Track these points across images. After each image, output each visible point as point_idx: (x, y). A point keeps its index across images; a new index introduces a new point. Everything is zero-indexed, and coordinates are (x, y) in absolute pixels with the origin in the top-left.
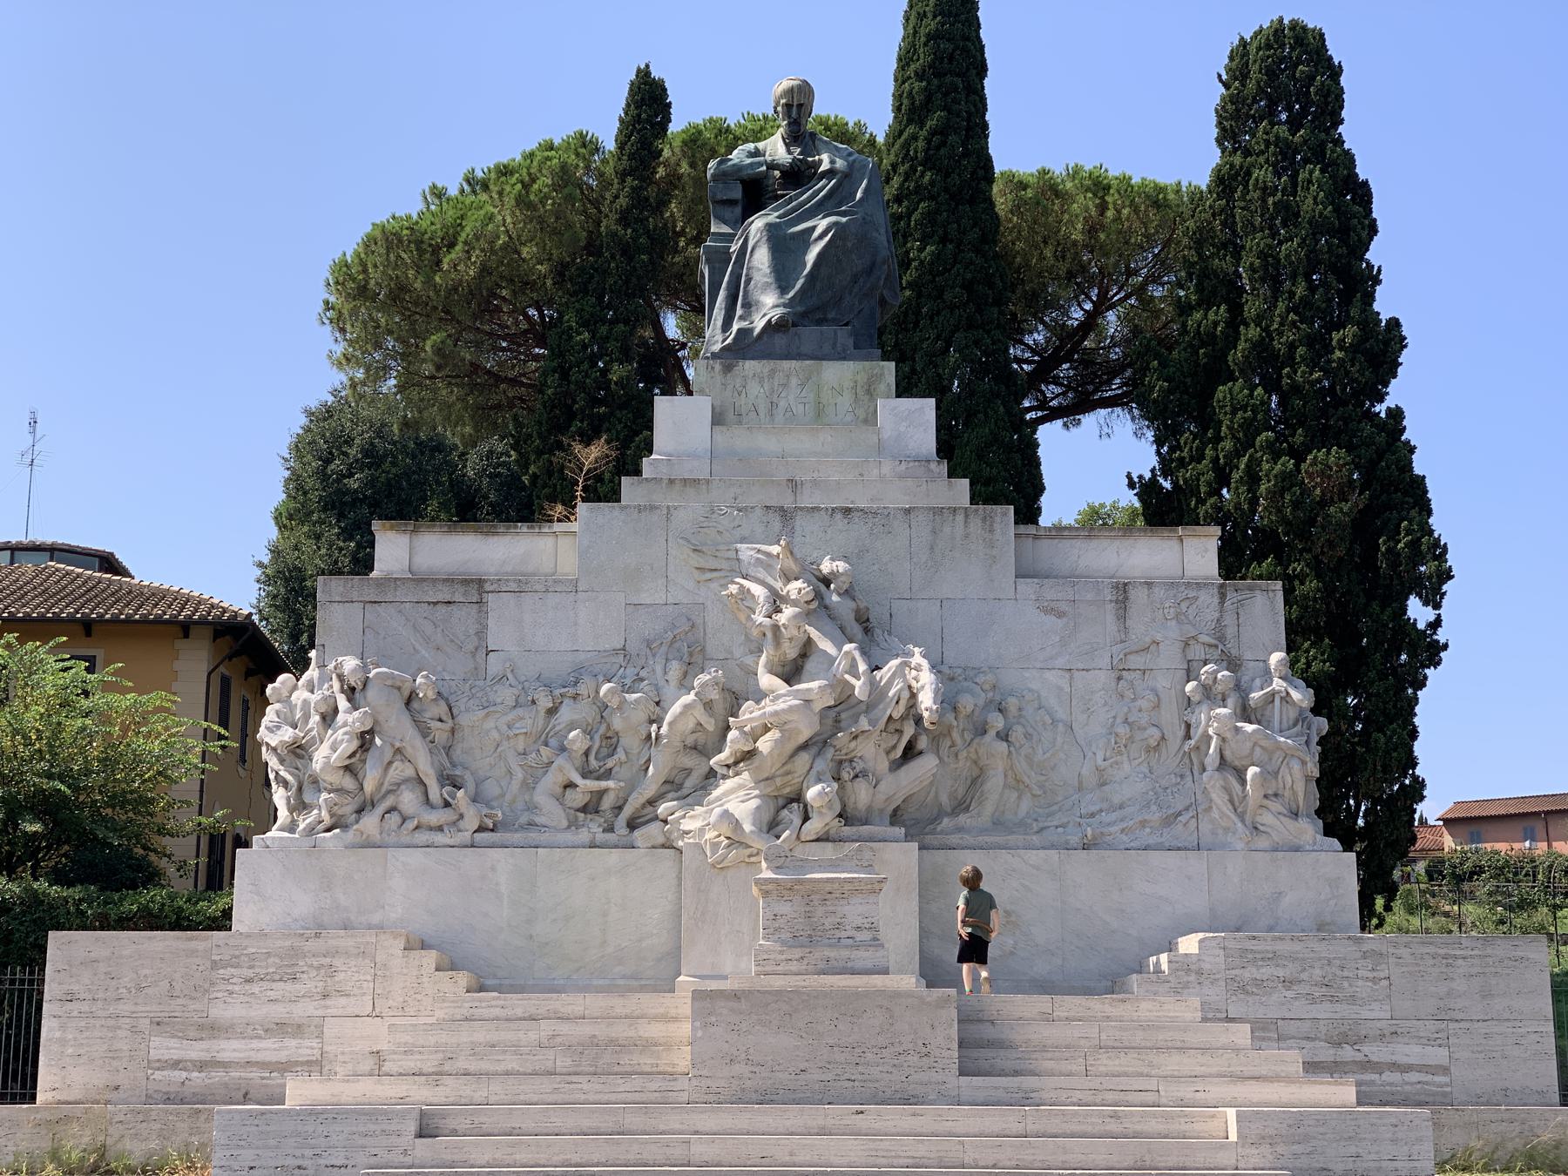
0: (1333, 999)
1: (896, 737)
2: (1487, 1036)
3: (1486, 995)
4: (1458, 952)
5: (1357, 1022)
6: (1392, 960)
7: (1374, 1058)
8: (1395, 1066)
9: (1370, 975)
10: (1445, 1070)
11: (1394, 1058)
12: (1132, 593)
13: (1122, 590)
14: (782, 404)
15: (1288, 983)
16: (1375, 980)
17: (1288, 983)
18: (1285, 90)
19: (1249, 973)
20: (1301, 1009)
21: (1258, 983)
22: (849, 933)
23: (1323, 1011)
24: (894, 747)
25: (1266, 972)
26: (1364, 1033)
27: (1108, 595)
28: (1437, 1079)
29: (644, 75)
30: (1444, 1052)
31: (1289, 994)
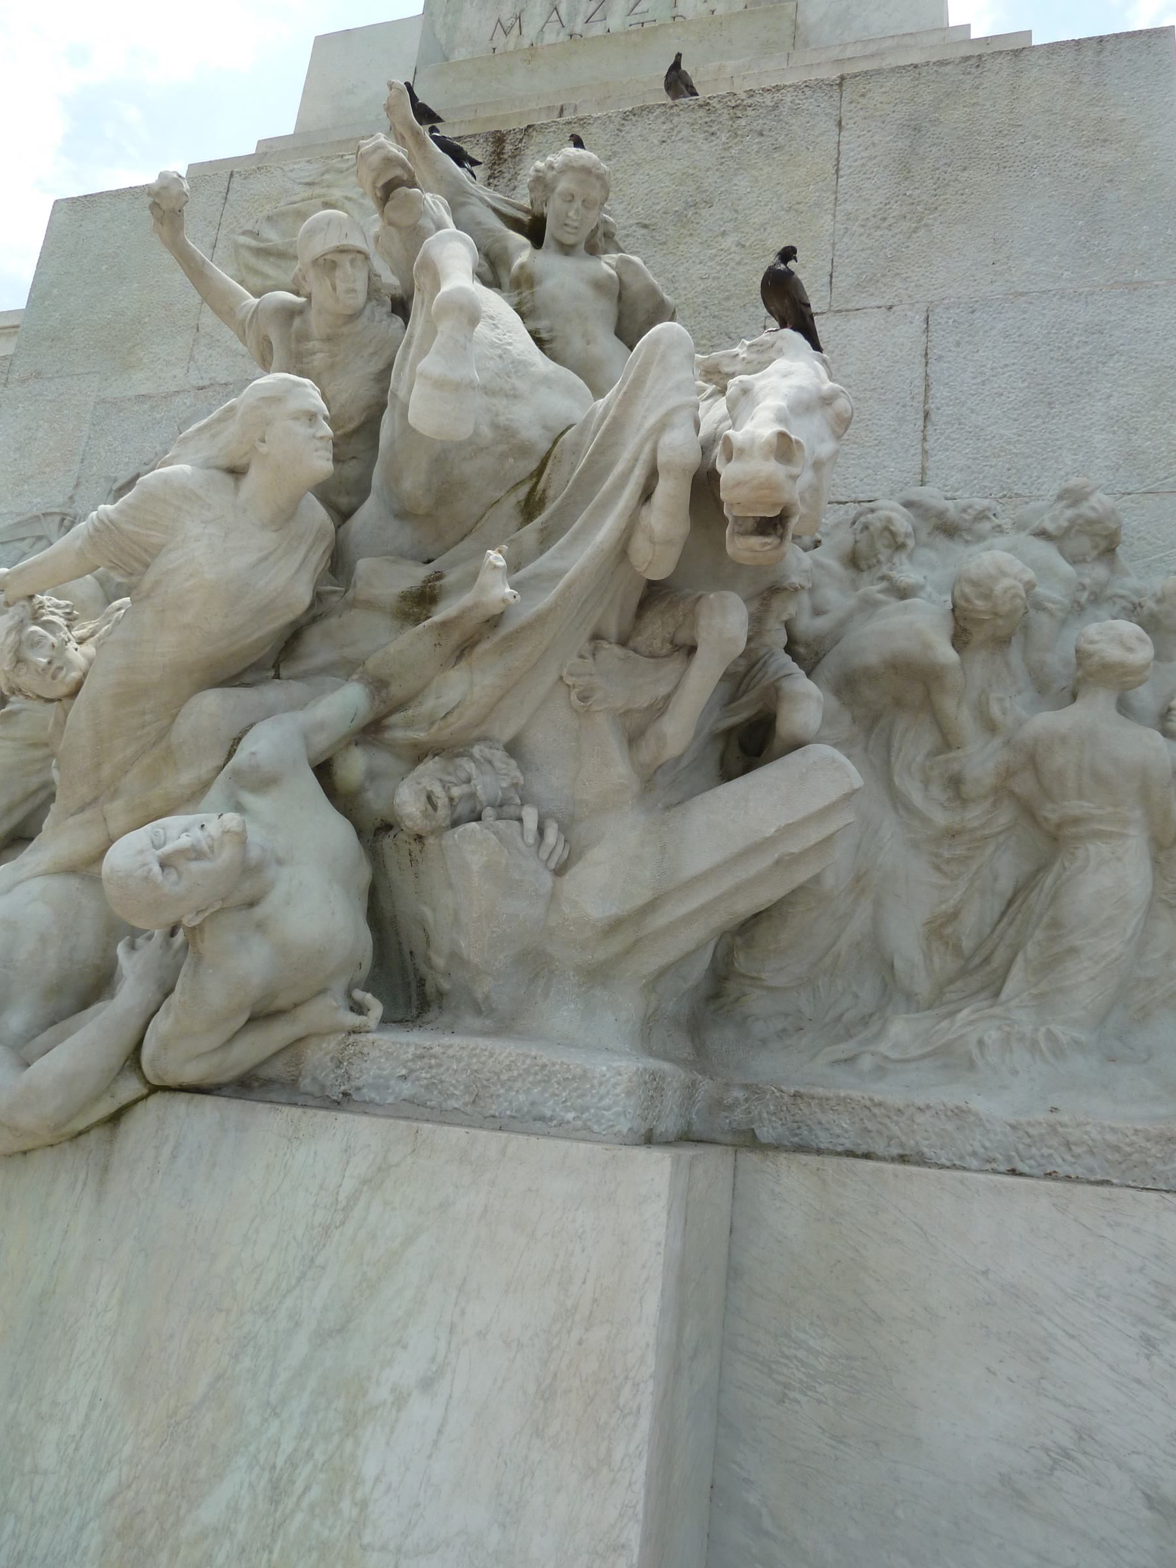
1: (672, 667)
24: (659, 709)
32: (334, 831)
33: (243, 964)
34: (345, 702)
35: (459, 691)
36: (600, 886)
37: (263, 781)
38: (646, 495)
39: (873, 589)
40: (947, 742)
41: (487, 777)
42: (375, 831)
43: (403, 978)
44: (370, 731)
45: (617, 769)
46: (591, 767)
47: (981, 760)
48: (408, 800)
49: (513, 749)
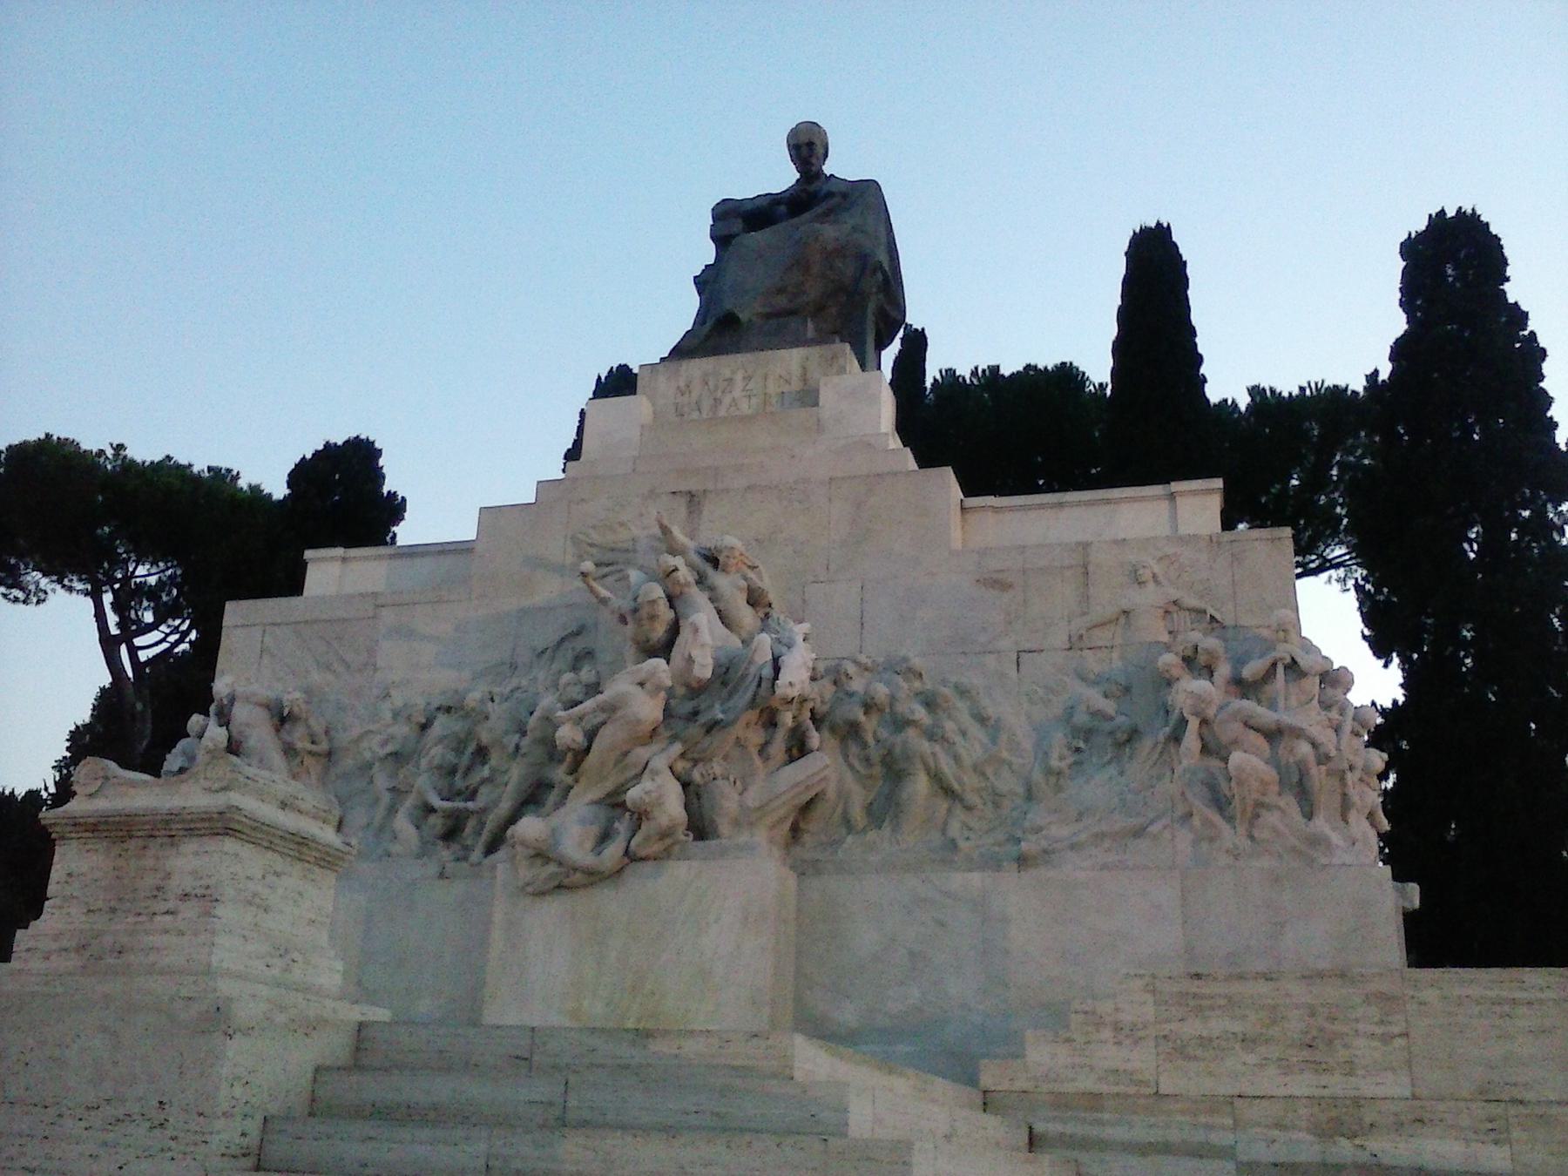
0: (1319, 1068)
4: (1518, 995)
5: (1357, 1102)
6: (1412, 1007)
9: (1379, 1030)
14: (727, 400)
15: (1248, 1042)
16: (1387, 1039)
17: (1248, 1042)
18: (1453, 267)
19: (1193, 1028)
20: (1270, 1082)
22: (170, 905)
23: (1303, 1085)
25: (1218, 1025)
26: (1368, 1120)
31: (1251, 1059)
38: (759, 685)
39: (841, 695)
40: (865, 745)
47: (875, 754)
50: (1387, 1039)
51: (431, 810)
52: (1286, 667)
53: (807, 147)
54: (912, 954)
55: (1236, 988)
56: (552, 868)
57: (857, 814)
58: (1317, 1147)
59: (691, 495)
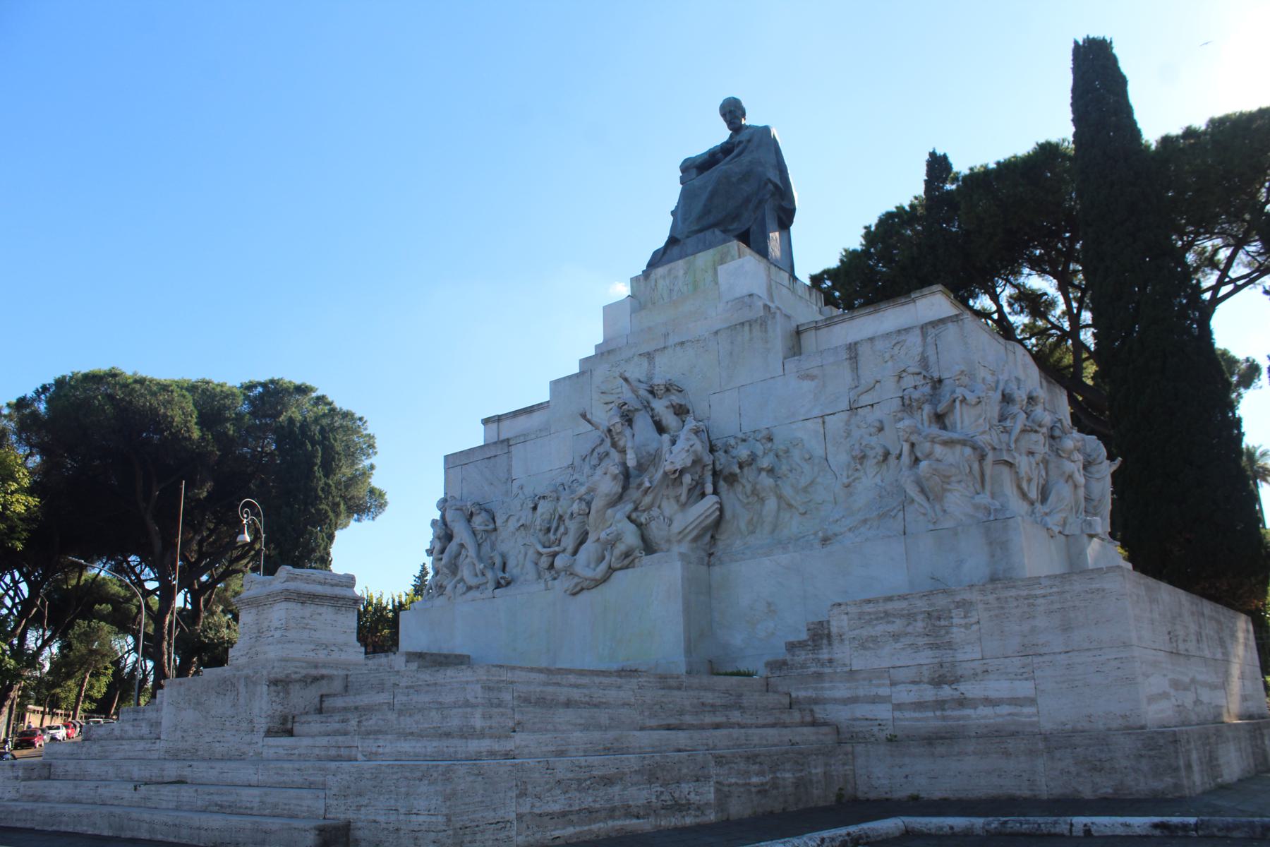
2: (1069, 666)
3: (1066, 628)
4: (1038, 592)
5: (953, 664)
6: (981, 606)
7: (969, 695)
8: (988, 702)
9: (963, 622)
10: (1032, 701)
11: (986, 693)
12: (864, 350)
13: (853, 348)
14: (676, 289)
15: (896, 637)
16: (967, 627)
17: (896, 637)
21: (875, 640)
26: (959, 673)
27: (844, 355)
28: (1026, 710)
29: (933, 155)
30: (1030, 684)
31: (899, 646)
32: (632, 527)
33: (621, 548)
34: (629, 507)
35: (647, 500)
36: (676, 527)
37: (619, 521)
41: (655, 512)
42: (639, 526)
43: (649, 547)
44: (636, 509)
45: (676, 507)
46: (669, 507)
48: (643, 520)
49: (659, 507)
50: (967, 627)
51: (540, 554)
52: (961, 402)
53: (732, 111)
54: (769, 604)
55: (890, 606)
56: (576, 580)
57: (743, 526)
58: (934, 692)
59: (649, 354)
